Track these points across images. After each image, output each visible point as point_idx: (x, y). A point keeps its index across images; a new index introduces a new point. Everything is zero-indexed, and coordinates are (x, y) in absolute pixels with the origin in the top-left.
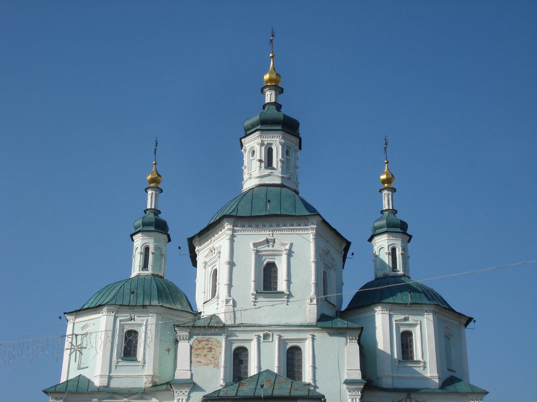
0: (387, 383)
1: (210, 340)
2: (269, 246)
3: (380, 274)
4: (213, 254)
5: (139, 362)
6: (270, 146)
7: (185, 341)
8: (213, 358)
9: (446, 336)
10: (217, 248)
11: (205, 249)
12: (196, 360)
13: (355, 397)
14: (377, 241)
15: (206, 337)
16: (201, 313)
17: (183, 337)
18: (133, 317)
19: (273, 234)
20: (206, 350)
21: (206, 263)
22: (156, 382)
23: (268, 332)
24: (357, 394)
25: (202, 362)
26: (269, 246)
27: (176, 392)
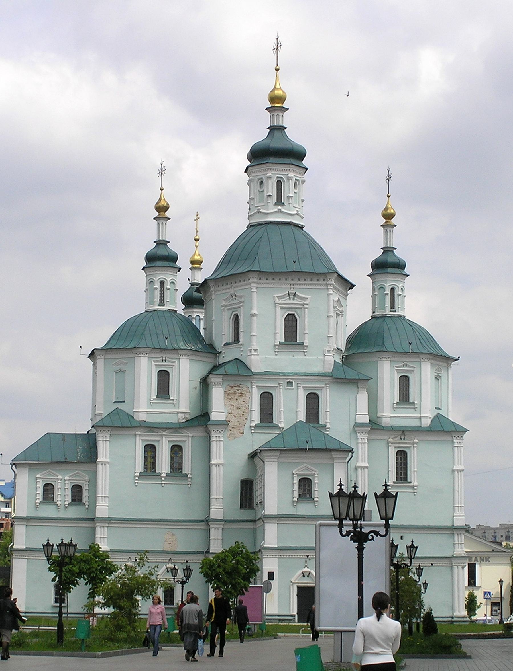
0: (386, 422)
1: (240, 386)
2: (290, 299)
3: (378, 313)
4: (234, 299)
5: (173, 400)
6: (279, 179)
7: (219, 386)
8: (244, 402)
9: (436, 378)
10: (241, 297)
11: (225, 291)
12: (229, 403)
13: (363, 437)
14: (376, 280)
15: (238, 383)
16: (221, 352)
17: (217, 383)
18: (164, 359)
19: (293, 288)
20: (237, 395)
21: (226, 306)
22: (187, 418)
23: (292, 381)
24: (365, 435)
25: (234, 405)
26: (290, 299)
27: (214, 431)
